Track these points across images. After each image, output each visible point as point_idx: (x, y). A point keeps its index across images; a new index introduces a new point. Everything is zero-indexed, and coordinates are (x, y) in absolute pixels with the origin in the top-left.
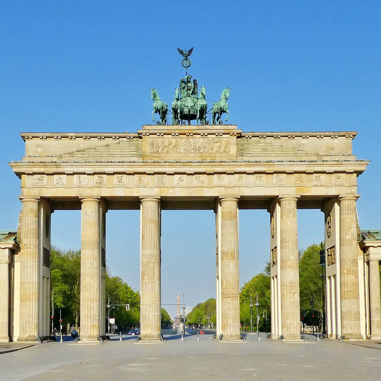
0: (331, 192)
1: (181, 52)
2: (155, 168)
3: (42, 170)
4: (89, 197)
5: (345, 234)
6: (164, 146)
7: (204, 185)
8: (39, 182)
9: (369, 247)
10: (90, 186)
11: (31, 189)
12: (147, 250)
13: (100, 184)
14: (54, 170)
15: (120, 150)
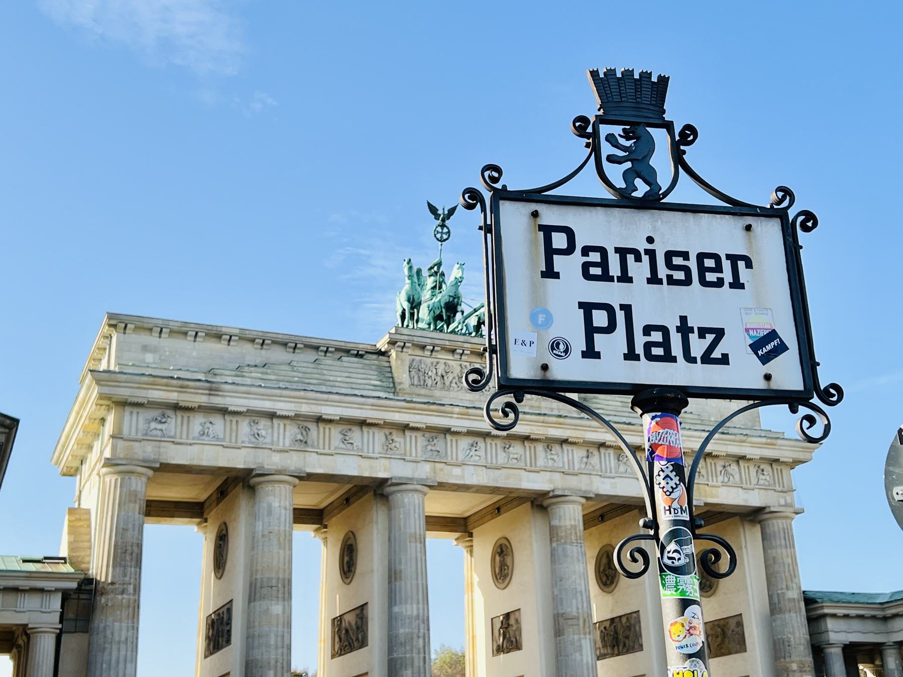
0: (754, 499)
1: (433, 210)
2: (429, 417)
3: (173, 397)
4: (279, 472)
5: (784, 586)
6: (439, 374)
7: (522, 465)
8: (159, 426)
9: (825, 616)
10: (281, 447)
11: (137, 444)
12: (409, 607)
13: (303, 443)
14: (203, 399)
15: (346, 375)
